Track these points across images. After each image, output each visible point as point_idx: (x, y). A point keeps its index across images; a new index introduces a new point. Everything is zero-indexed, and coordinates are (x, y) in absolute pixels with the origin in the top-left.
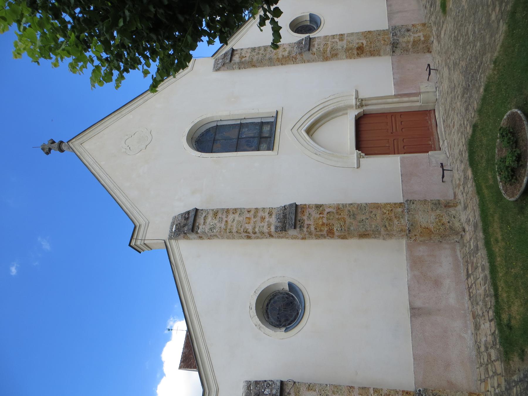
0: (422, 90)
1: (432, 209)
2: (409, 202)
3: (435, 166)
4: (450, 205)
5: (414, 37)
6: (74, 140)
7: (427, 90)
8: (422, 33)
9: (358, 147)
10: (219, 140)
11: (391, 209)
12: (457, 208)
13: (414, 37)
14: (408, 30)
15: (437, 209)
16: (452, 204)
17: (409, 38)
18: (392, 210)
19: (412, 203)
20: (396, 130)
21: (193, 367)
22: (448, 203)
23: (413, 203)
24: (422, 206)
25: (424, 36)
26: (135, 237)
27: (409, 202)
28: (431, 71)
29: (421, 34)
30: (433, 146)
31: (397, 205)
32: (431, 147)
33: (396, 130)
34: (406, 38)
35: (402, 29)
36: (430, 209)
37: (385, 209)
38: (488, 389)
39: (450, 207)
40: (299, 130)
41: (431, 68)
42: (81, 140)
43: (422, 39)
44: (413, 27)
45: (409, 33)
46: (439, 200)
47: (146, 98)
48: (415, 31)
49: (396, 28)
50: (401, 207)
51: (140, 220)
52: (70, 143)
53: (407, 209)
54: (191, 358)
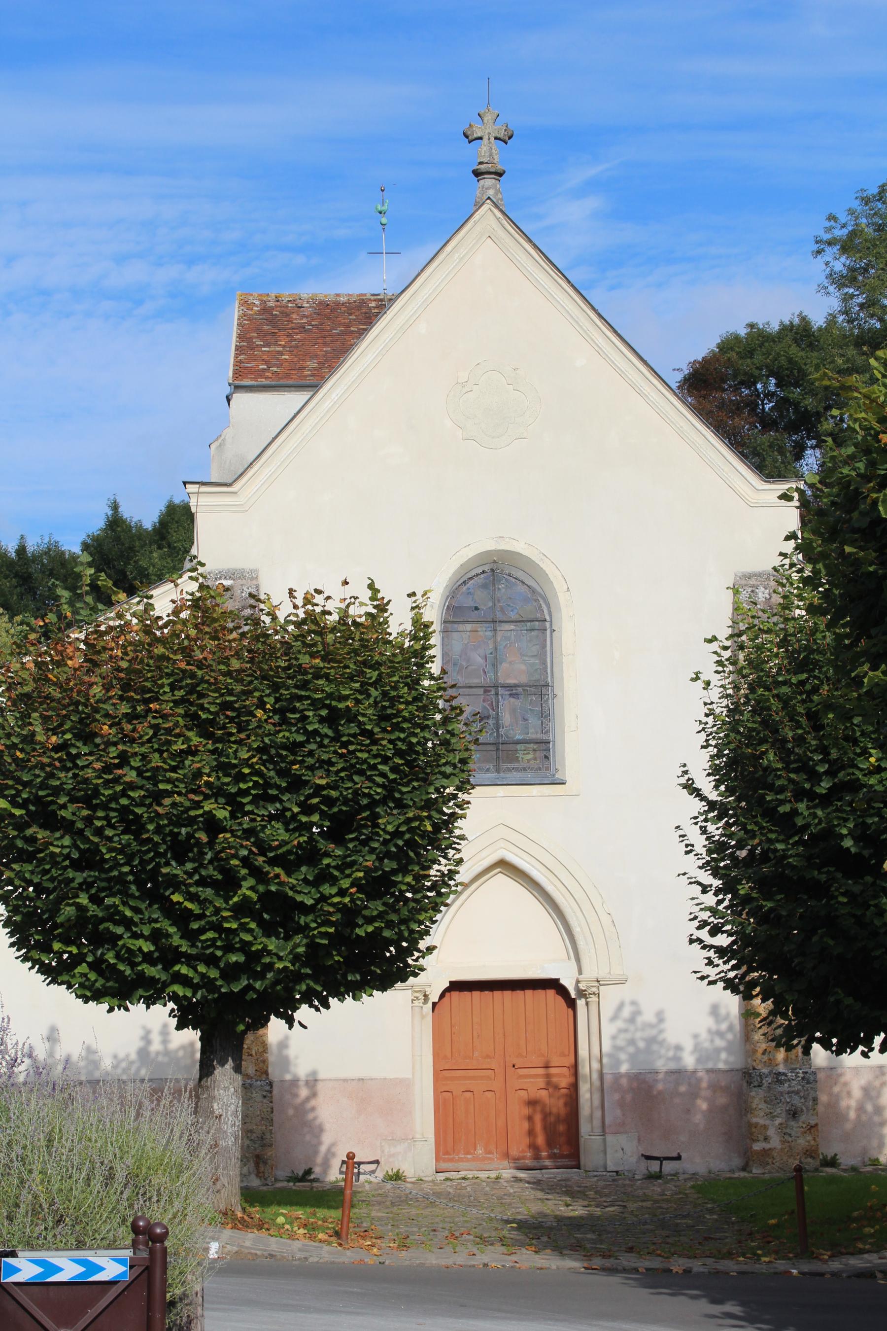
0: (610, 1138)
1: (251, 1131)
2: (268, 1088)
3: (383, 1152)
4: (261, 1165)
5: (765, 1127)
6: (499, 214)
7: (609, 1150)
8: (779, 1147)
9: (456, 986)
10: (495, 636)
11: (253, 1053)
12: (253, 1177)
13: (765, 1127)
14: (794, 1114)
15: (251, 1140)
16: (262, 1169)
17: (762, 1114)
18: (251, 1055)
19: (264, 1093)
20: (521, 1077)
21: (241, 362)
22: (265, 1163)
23: (265, 1097)
24: (259, 1113)
25: (766, 1153)
26: (204, 489)
27: (268, 1088)
28: (659, 1162)
29: (775, 1142)
30: (469, 1156)
31: (261, 1065)
32: (468, 1153)
33: (521, 1077)
34: (763, 1106)
35: (801, 1098)
36: (250, 1128)
37: (253, 1042)
38: (20, 1254)
39: (257, 1165)
40: (502, 844)
41: (664, 1162)
42: (501, 233)
43: (757, 1147)
44: (804, 1126)
45: (784, 1115)
46: (271, 1145)
47: (647, 389)
48: (788, 1131)
49: (808, 1083)
50: (258, 1073)
51: (247, 488)
52: (488, 205)
53: (251, 1085)
54: (276, 344)
